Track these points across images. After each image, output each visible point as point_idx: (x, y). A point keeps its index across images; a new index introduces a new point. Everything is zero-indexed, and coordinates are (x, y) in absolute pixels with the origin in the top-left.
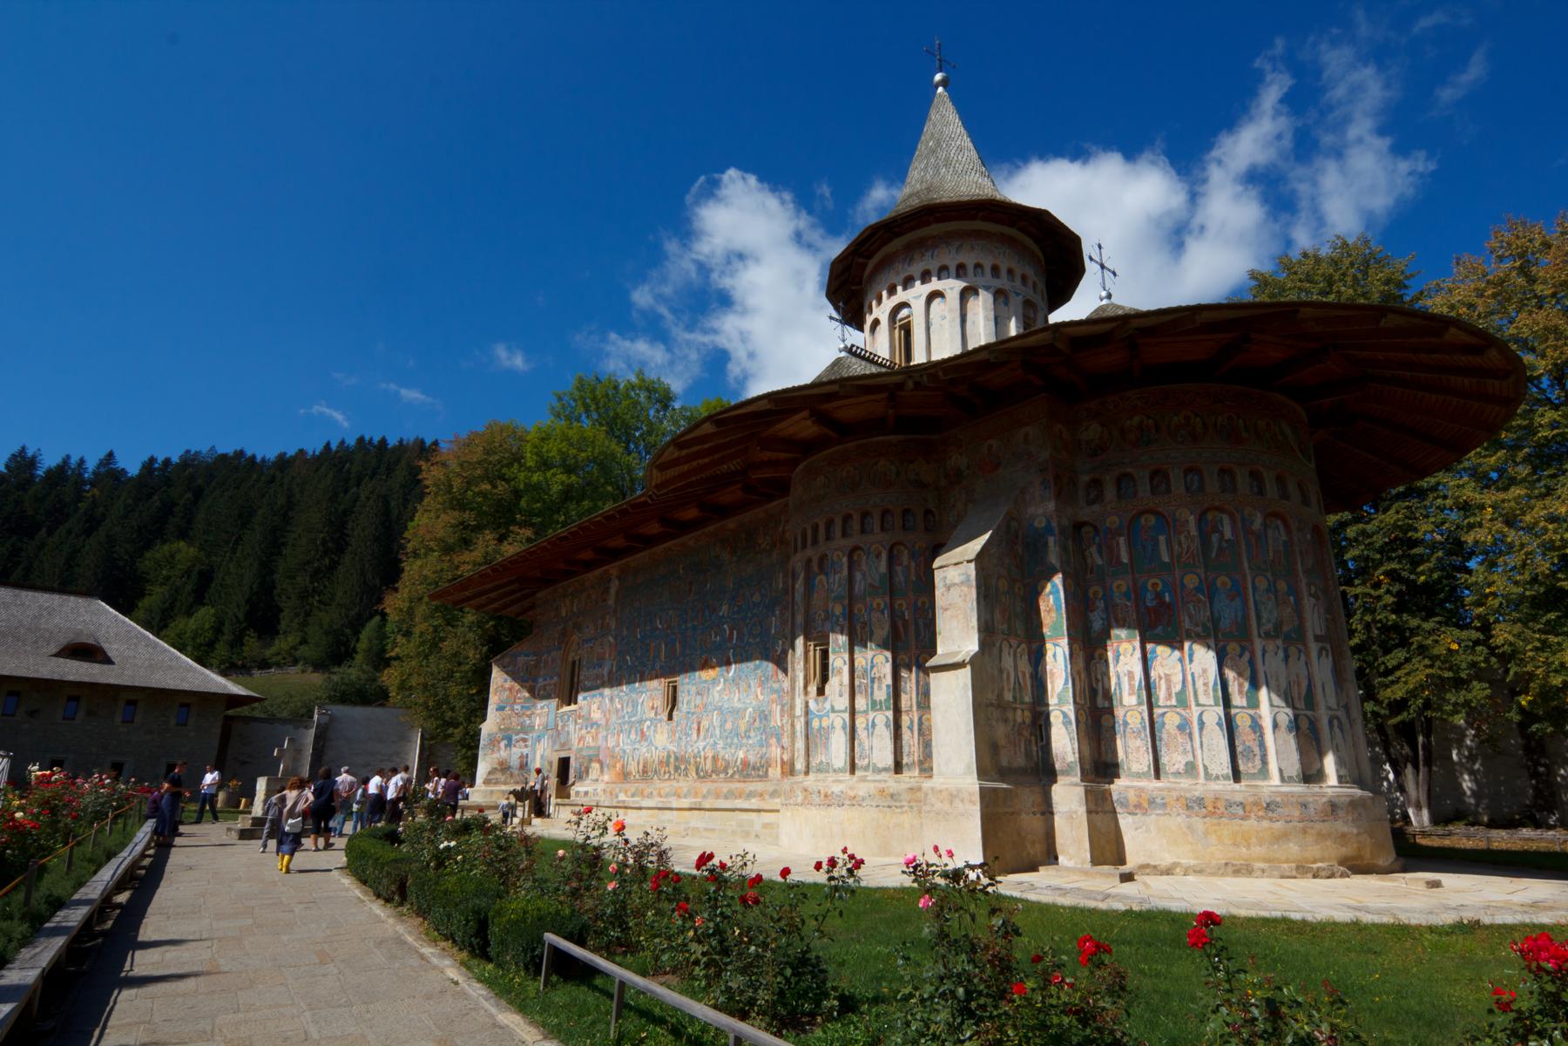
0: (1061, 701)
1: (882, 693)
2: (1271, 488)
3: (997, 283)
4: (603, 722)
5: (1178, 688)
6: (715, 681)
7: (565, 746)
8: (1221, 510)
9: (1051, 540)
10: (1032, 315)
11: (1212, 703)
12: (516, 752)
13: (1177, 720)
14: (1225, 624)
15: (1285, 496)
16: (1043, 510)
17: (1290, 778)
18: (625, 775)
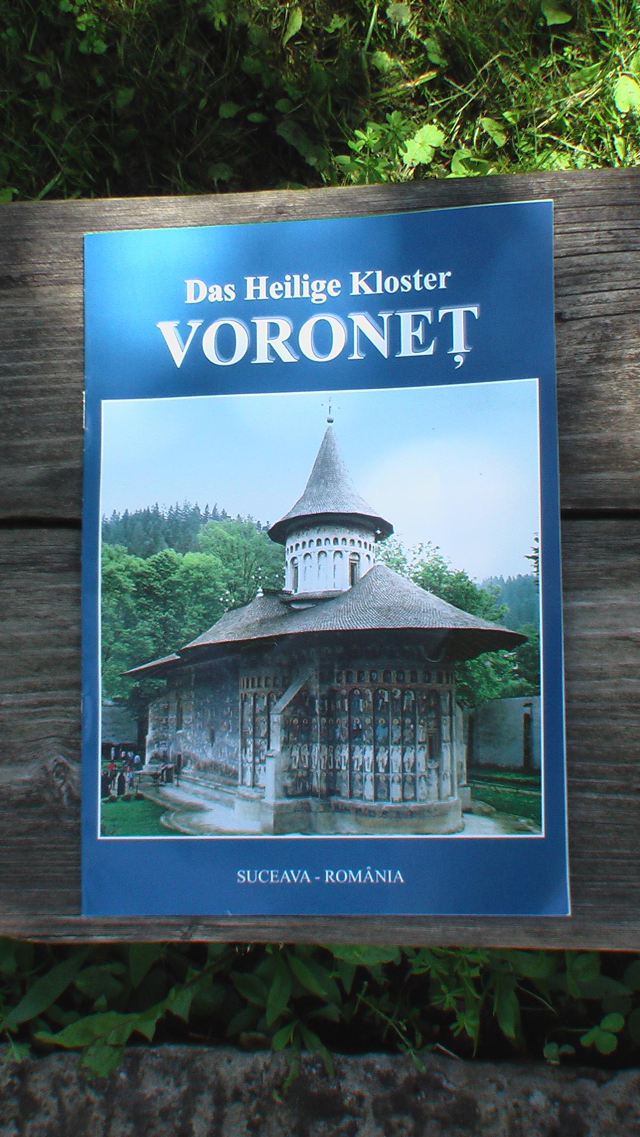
2: (408, 678)
3: (337, 548)
4: (191, 741)
5: (360, 764)
6: (226, 732)
7: (179, 749)
9: (317, 701)
10: (357, 558)
11: (369, 771)
12: (162, 749)
14: (380, 738)
16: (316, 689)
17: (396, 802)
18: (198, 768)
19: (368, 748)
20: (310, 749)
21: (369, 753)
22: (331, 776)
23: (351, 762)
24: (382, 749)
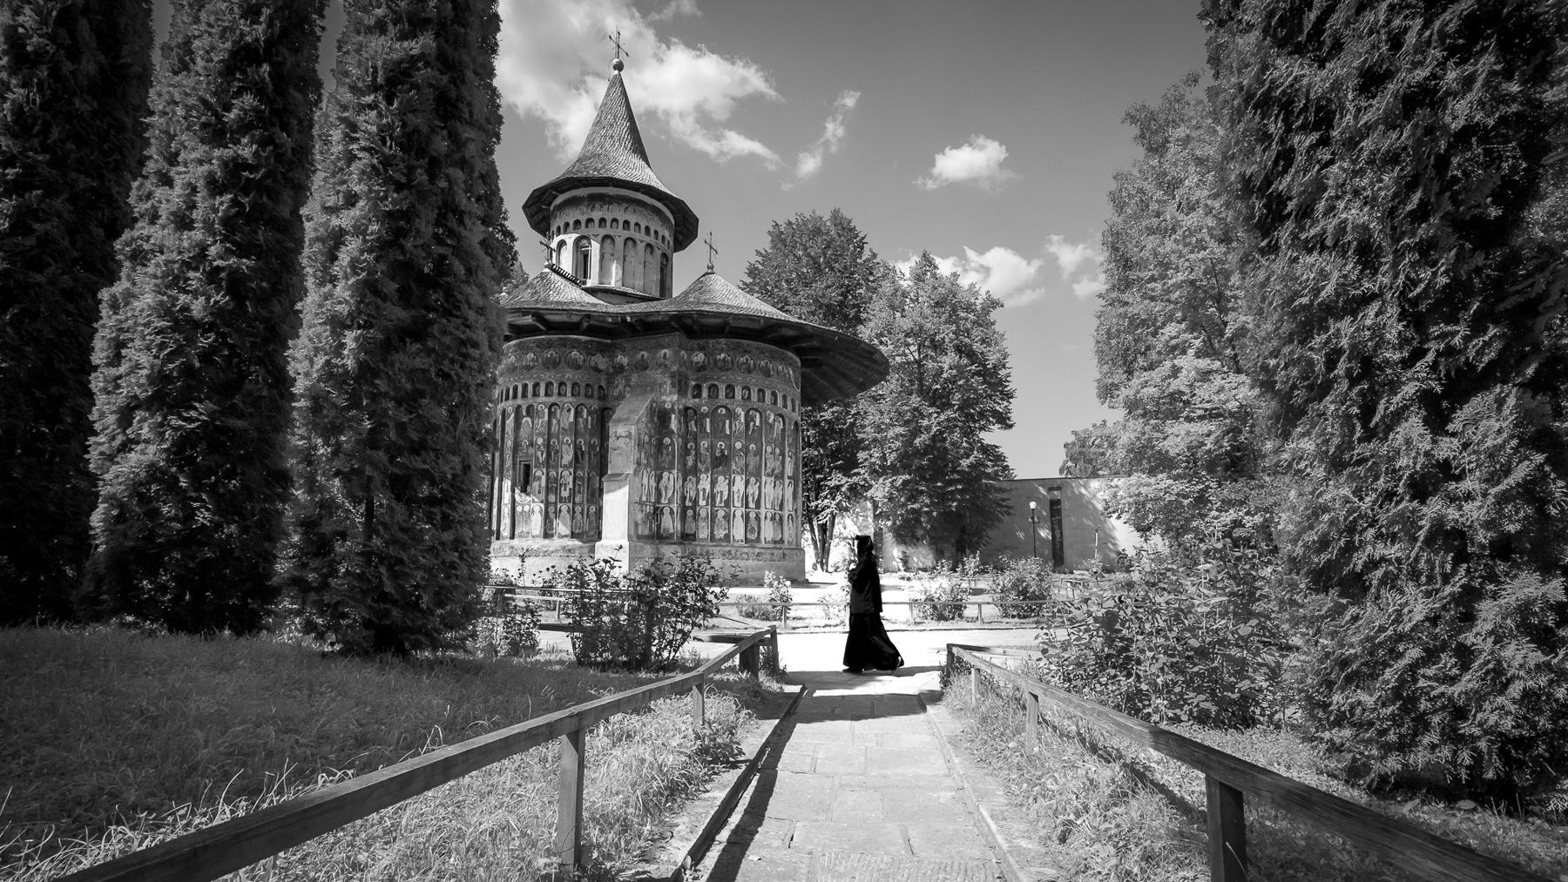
0: (670, 501)
1: (565, 494)
3: (648, 239)
5: (725, 498)
8: (756, 410)
13: (723, 513)
14: (751, 468)
15: (785, 406)
16: (670, 399)
19: (738, 478)
20: (659, 479)
21: (739, 484)
22: (688, 510)
23: (713, 497)
24: (753, 480)
